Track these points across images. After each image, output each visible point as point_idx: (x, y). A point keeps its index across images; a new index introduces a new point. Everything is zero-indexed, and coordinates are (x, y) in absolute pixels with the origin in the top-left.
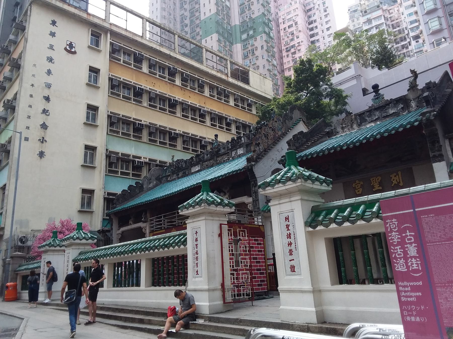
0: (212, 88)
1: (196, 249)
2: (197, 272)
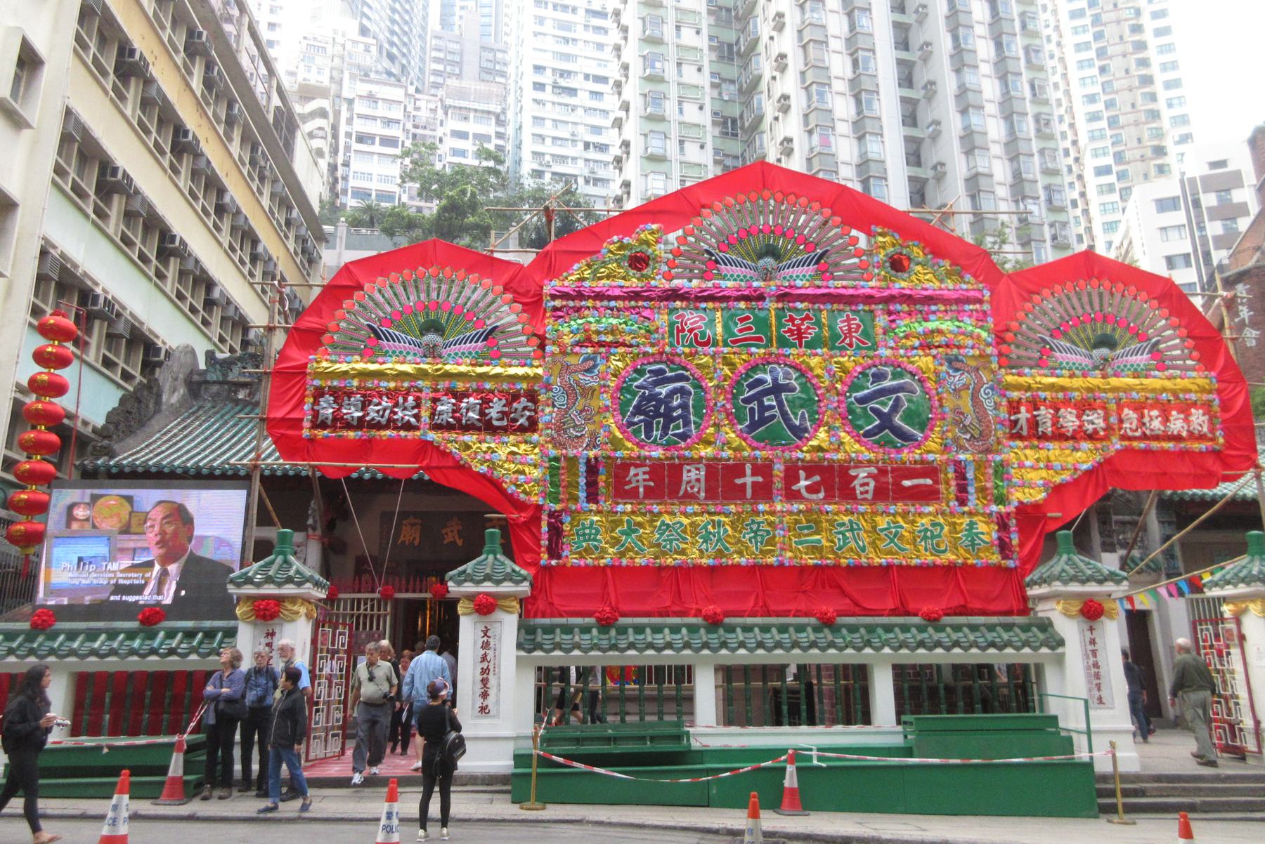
0: (246, 138)
2: (1100, 699)
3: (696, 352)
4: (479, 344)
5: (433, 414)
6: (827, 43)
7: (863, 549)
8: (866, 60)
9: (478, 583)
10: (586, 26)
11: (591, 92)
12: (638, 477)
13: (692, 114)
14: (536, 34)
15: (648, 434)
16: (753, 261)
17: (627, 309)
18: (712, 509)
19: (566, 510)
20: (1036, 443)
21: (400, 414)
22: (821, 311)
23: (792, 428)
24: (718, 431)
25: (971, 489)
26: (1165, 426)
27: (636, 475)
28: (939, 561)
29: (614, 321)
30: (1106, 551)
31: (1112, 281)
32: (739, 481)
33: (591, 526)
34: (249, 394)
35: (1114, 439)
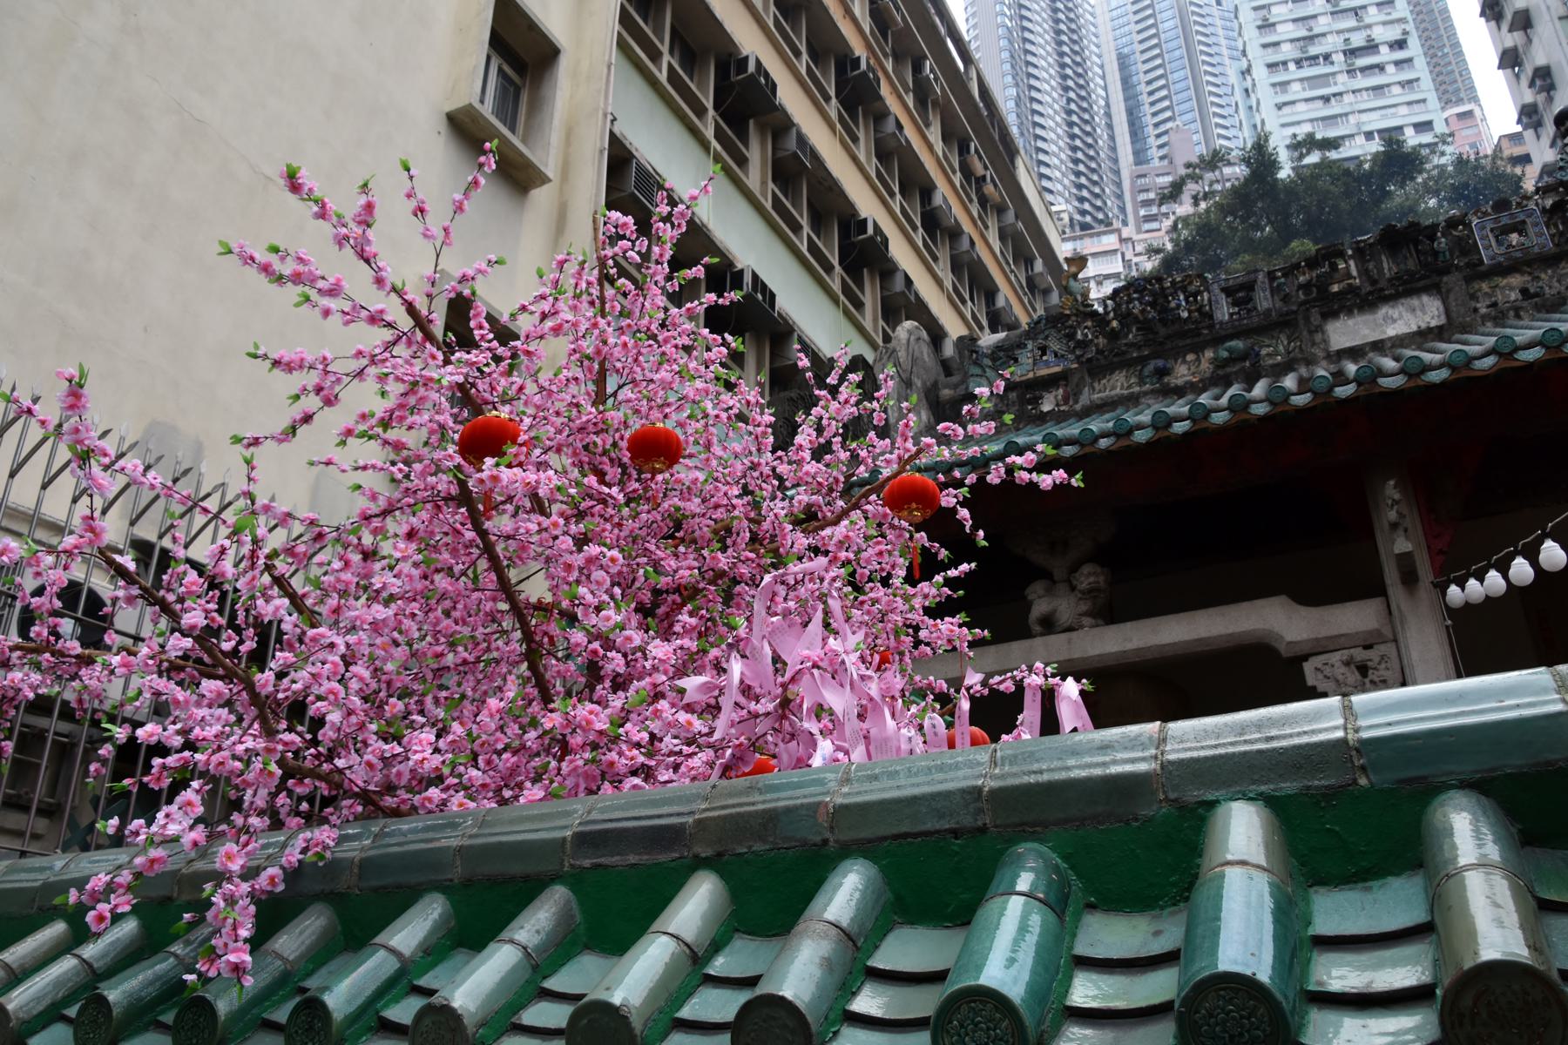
10: (1351, 72)
34: (1066, 400)
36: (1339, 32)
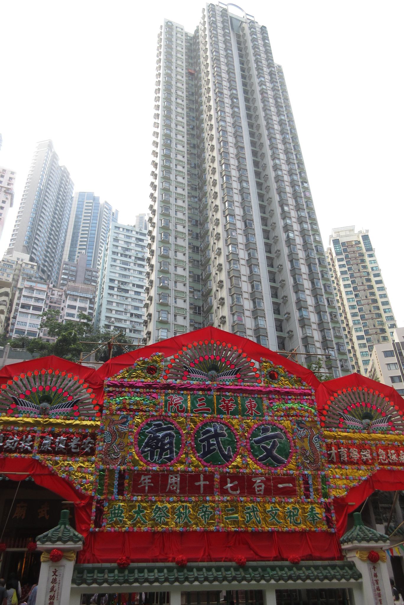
1: (376, 586)
3: (178, 416)
4: (69, 408)
5: (40, 445)
6: (240, 278)
7: (259, 522)
8: (257, 286)
9: (54, 542)
10: (135, 264)
11: (135, 292)
12: (146, 480)
13: (180, 303)
14: (112, 266)
15: (152, 458)
16: (206, 372)
17: (145, 393)
18: (183, 499)
19: (106, 499)
20: (340, 466)
21: (23, 445)
22: (238, 397)
23: (224, 455)
24: (187, 457)
25: (311, 490)
26: (399, 458)
27: (144, 480)
28: (297, 529)
29: (138, 399)
30: (378, 523)
31: (368, 387)
32: (197, 484)
33: (119, 509)
35: (376, 465)
36: (136, 251)
